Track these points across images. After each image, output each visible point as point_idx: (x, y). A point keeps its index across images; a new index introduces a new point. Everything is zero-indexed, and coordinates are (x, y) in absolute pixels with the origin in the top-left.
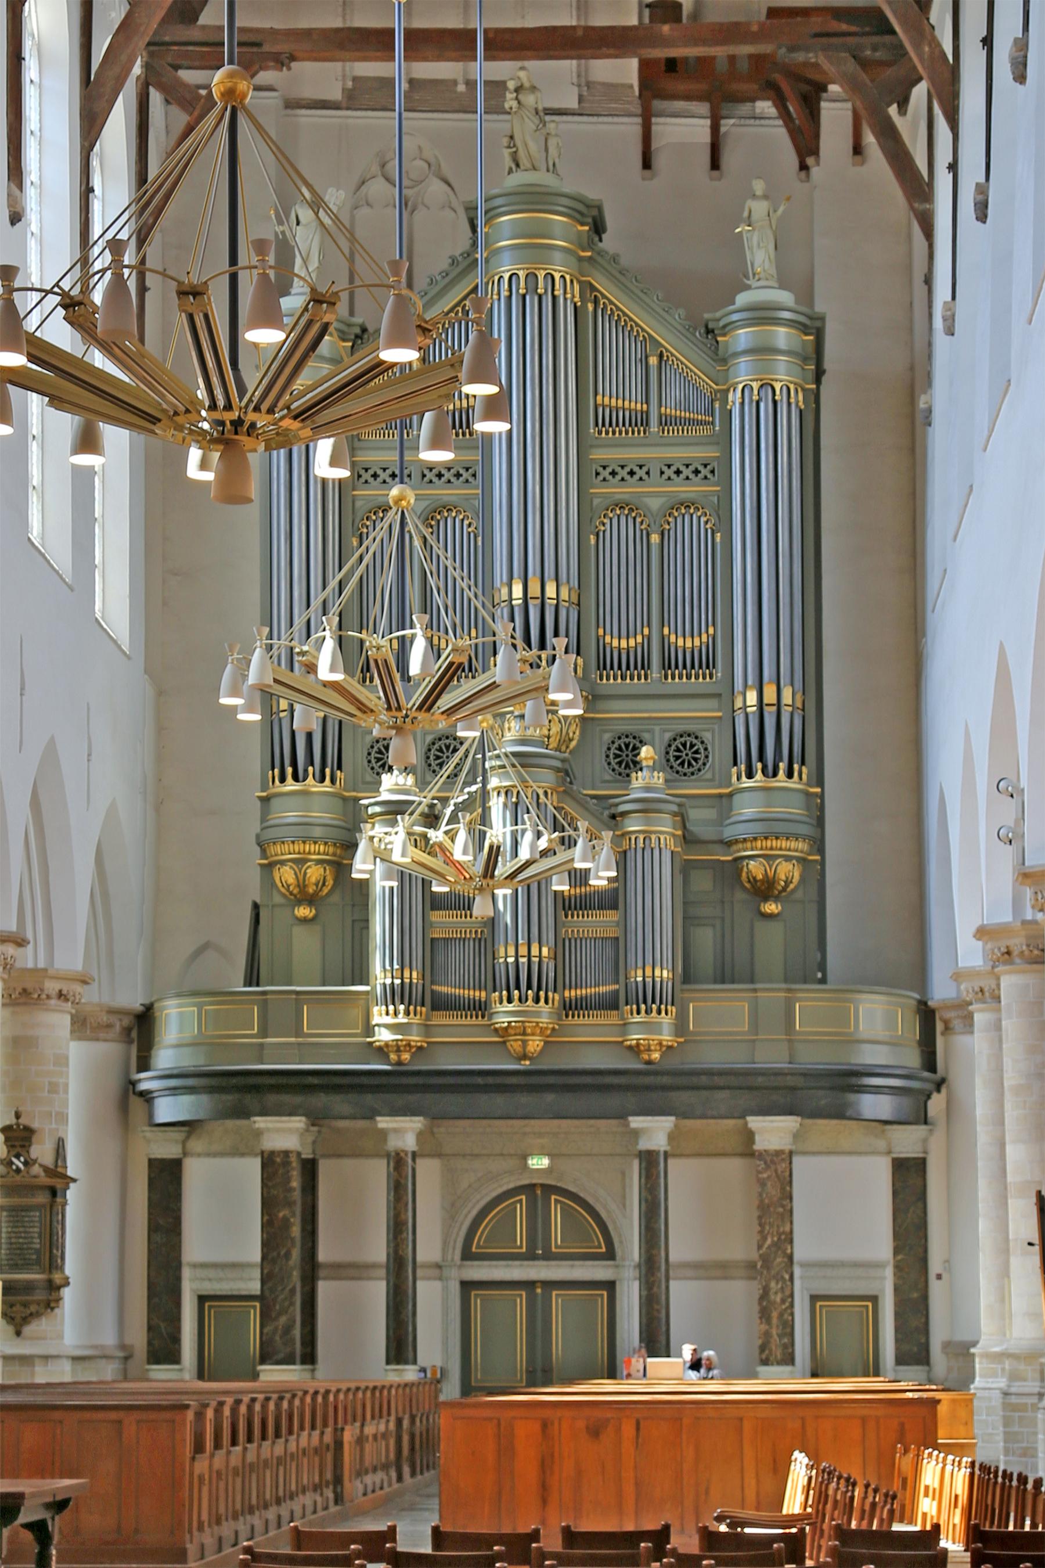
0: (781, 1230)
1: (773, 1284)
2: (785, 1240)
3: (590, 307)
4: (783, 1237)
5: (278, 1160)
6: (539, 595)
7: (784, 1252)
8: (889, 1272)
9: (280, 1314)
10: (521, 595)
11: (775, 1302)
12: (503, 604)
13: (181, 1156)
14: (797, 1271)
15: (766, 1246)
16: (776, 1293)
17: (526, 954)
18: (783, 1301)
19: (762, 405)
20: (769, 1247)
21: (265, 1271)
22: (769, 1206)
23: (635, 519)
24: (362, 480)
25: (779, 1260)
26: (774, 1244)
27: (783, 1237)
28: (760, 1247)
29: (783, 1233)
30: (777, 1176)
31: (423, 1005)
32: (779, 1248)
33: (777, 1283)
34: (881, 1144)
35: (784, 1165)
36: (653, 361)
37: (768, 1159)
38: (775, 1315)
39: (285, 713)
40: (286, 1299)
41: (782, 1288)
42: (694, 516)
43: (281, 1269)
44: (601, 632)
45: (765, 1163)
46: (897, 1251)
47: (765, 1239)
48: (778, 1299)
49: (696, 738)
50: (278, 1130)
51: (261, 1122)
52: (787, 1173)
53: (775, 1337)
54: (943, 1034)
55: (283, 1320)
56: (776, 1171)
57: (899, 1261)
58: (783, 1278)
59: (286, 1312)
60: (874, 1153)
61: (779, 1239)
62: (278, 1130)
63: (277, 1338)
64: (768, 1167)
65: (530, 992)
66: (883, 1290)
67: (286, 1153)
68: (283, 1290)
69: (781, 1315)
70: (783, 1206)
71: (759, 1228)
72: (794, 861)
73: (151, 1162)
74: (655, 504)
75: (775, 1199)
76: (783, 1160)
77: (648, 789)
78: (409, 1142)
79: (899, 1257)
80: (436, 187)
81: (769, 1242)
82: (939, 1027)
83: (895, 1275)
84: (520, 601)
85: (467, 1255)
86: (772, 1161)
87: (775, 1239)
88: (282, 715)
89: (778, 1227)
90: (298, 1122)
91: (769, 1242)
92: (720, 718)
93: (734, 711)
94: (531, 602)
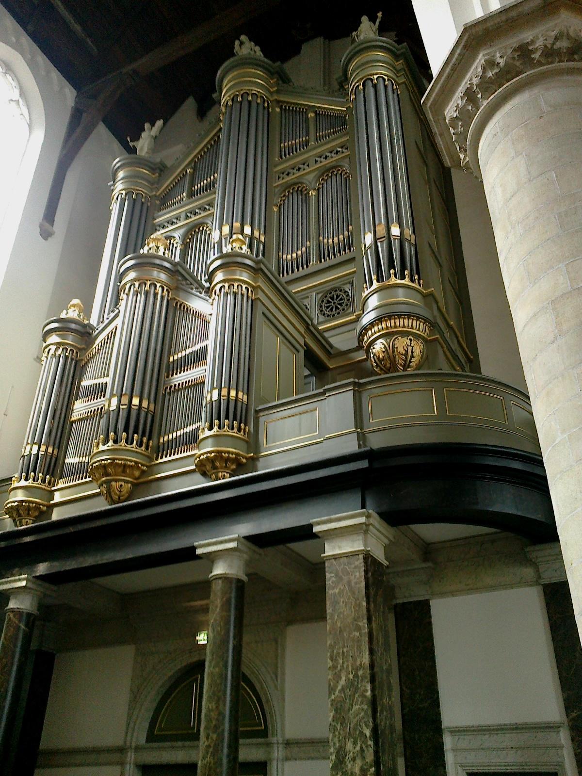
1: (349, 746)
2: (364, 677)
3: (278, 110)
4: (360, 673)
7: (363, 696)
8: (564, 737)
14: (448, 741)
15: (339, 688)
20: (343, 690)
23: (301, 191)
25: (356, 707)
27: (360, 673)
28: (331, 690)
32: (356, 689)
33: (355, 743)
34: (528, 572)
36: (311, 115)
44: (281, 254)
45: (336, 575)
46: (569, 706)
47: (338, 677)
49: (341, 291)
56: (349, 582)
57: (573, 719)
60: (522, 583)
61: (356, 676)
66: (561, 765)
70: (359, 629)
71: (330, 664)
72: (410, 337)
74: (311, 177)
75: (349, 620)
79: (574, 715)
81: (343, 682)
83: (573, 740)
85: (151, 737)
87: (351, 676)
89: (355, 660)
91: (343, 682)
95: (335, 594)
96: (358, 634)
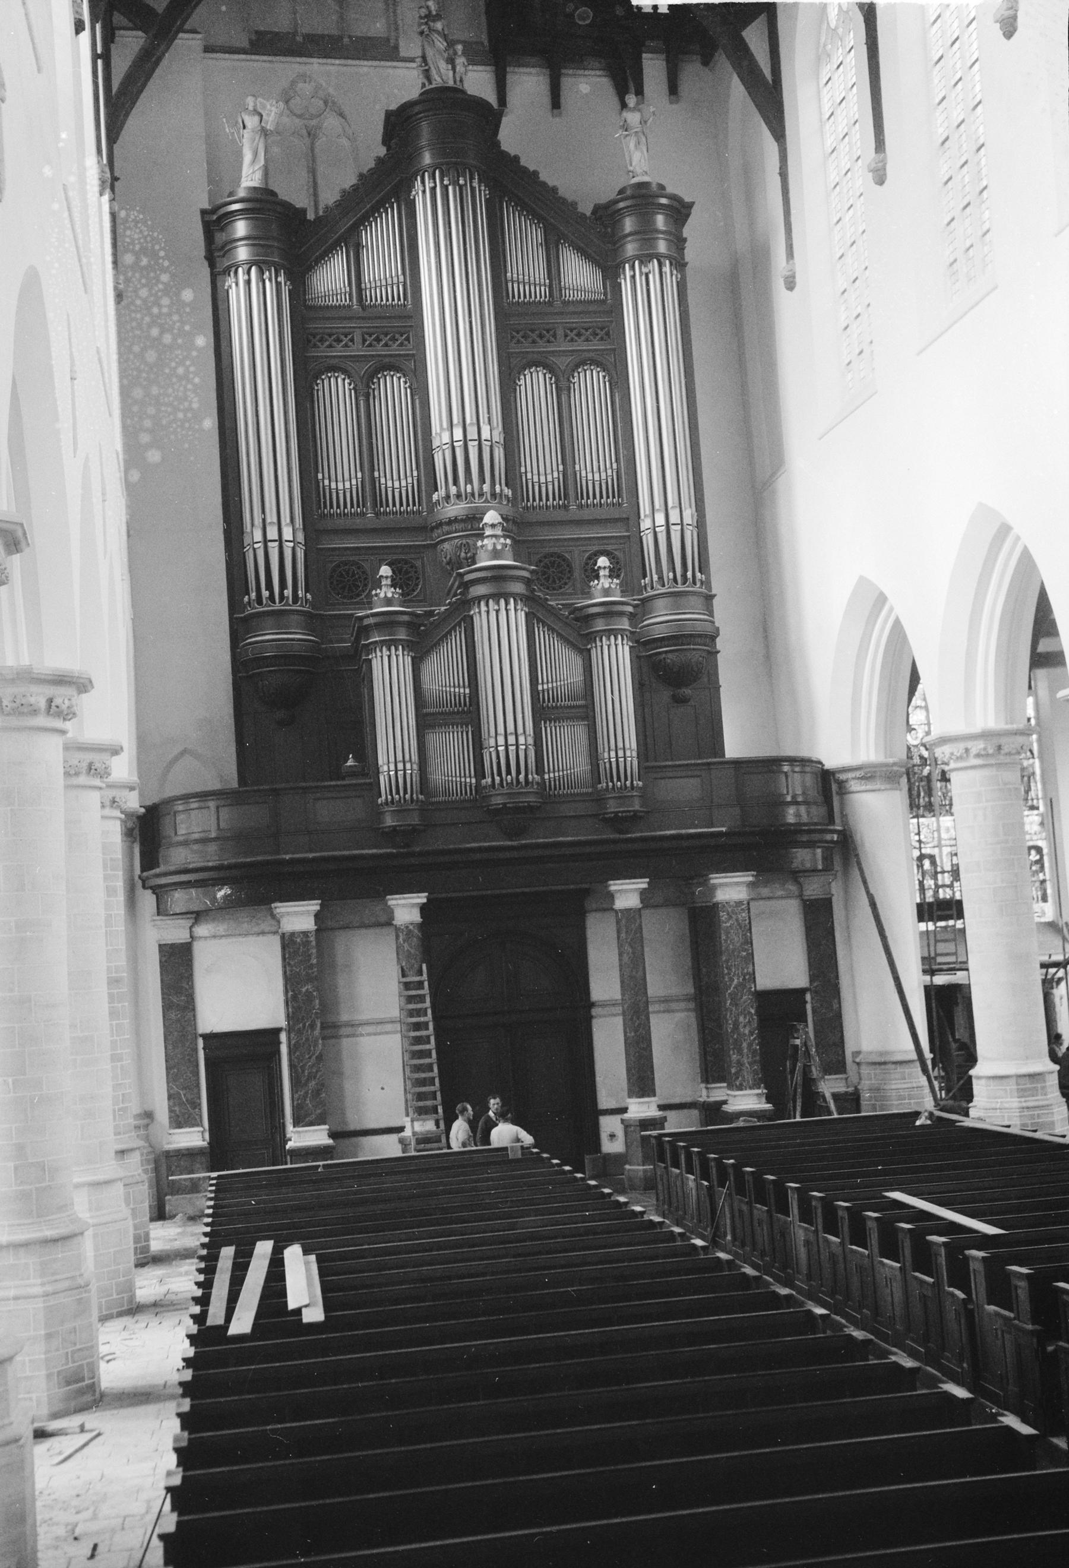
0: (745, 971)
1: (741, 1019)
4: (747, 977)
5: (298, 940)
6: (476, 437)
9: (309, 1079)
10: (461, 438)
11: (745, 1034)
12: (444, 447)
13: (190, 940)
16: (745, 1026)
17: (514, 742)
18: (751, 1033)
19: (651, 276)
21: (293, 1042)
22: (733, 951)
24: (311, 345)
26: (740, 984)
27: (747, 977)
29: (748, 973)
30: (739, 924)
31: (421, 794)
33: (745, 1017)
35: (744, 915)
37: (730, 910)
38: (745, 1045)
39: (260, 544)
40: (313, 1065)
41: (749, 1022)
42: (594, 371)
43: (307, 1039)
45: (728, 914)
48: (747, 1032)
50: (296, 913)
51: (282, 908)
52: (747, 922)
53: (747, 1065)
54: (837, 793)
55: (312, 1084)
56: (737, 920)
58: (750, 1013)
59: (315, 1077)
61: (744, 979)
62: (296, 913)
63: (308, 1102)
64: (730, 917)
65: (509, 777)
67: (305, 934)
68: (310, 1058)
69: (750, 1045)
70: (746, 950)
73: (162, 947)
76: (742, 909)
77: (607, 592)
78: (416, 917)
80: (331, 122)
82: (834, 787)
84: (461, 443)
86: (733, 911)
88: (256, 546)
90: (314, 906)
92: (629, 537)
93: (640, 532)
94: (470, 444)
95: (727, 927)
96: (745, 954)
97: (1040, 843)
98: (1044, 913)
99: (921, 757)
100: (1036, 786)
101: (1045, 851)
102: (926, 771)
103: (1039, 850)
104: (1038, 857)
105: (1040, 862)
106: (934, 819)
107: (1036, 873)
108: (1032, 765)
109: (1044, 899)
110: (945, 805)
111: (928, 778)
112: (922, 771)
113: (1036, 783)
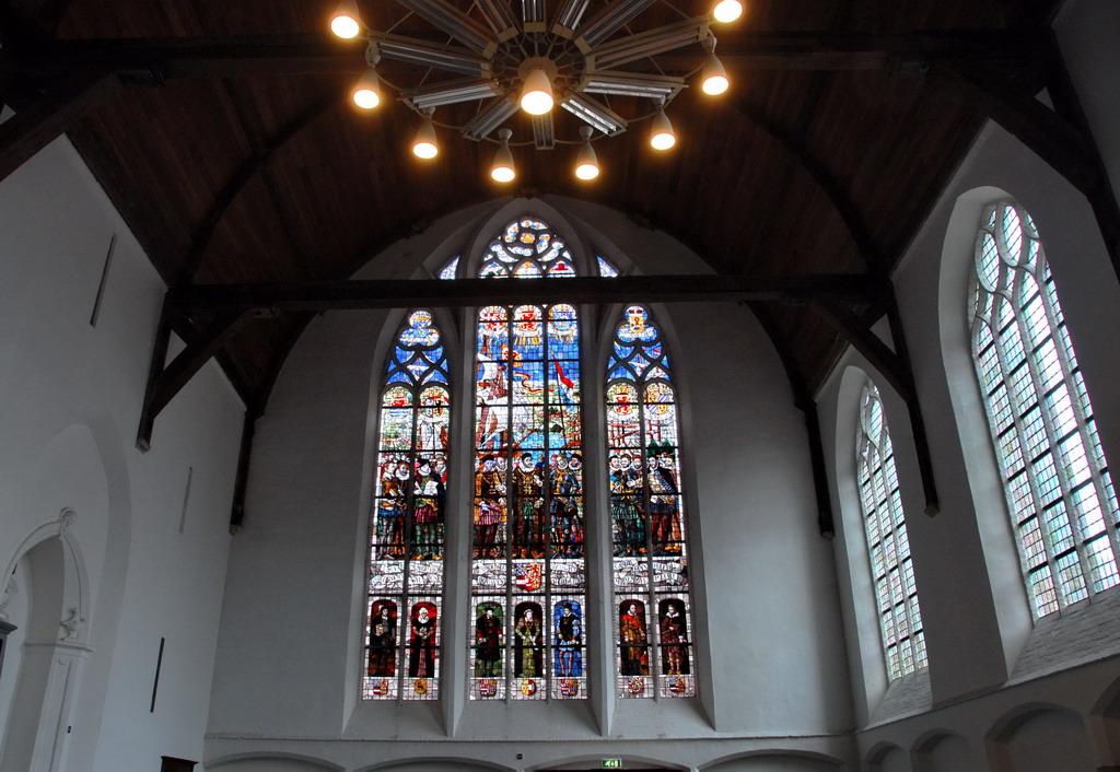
97: (680, 596)
98: (682, 687)
99: (534, 486)
100: (679, 527)
101: (687, 607)
102: (539, 503)
103: (679, 605)
104: (677, 615)
105: (681, 621)
106: (543, 561)
107: (675, 634)
108: (675, 503)
109: (685, 670)
110: (560, 544)
111: (541, 512)
112: (533, 503)
113: (679, 523)
